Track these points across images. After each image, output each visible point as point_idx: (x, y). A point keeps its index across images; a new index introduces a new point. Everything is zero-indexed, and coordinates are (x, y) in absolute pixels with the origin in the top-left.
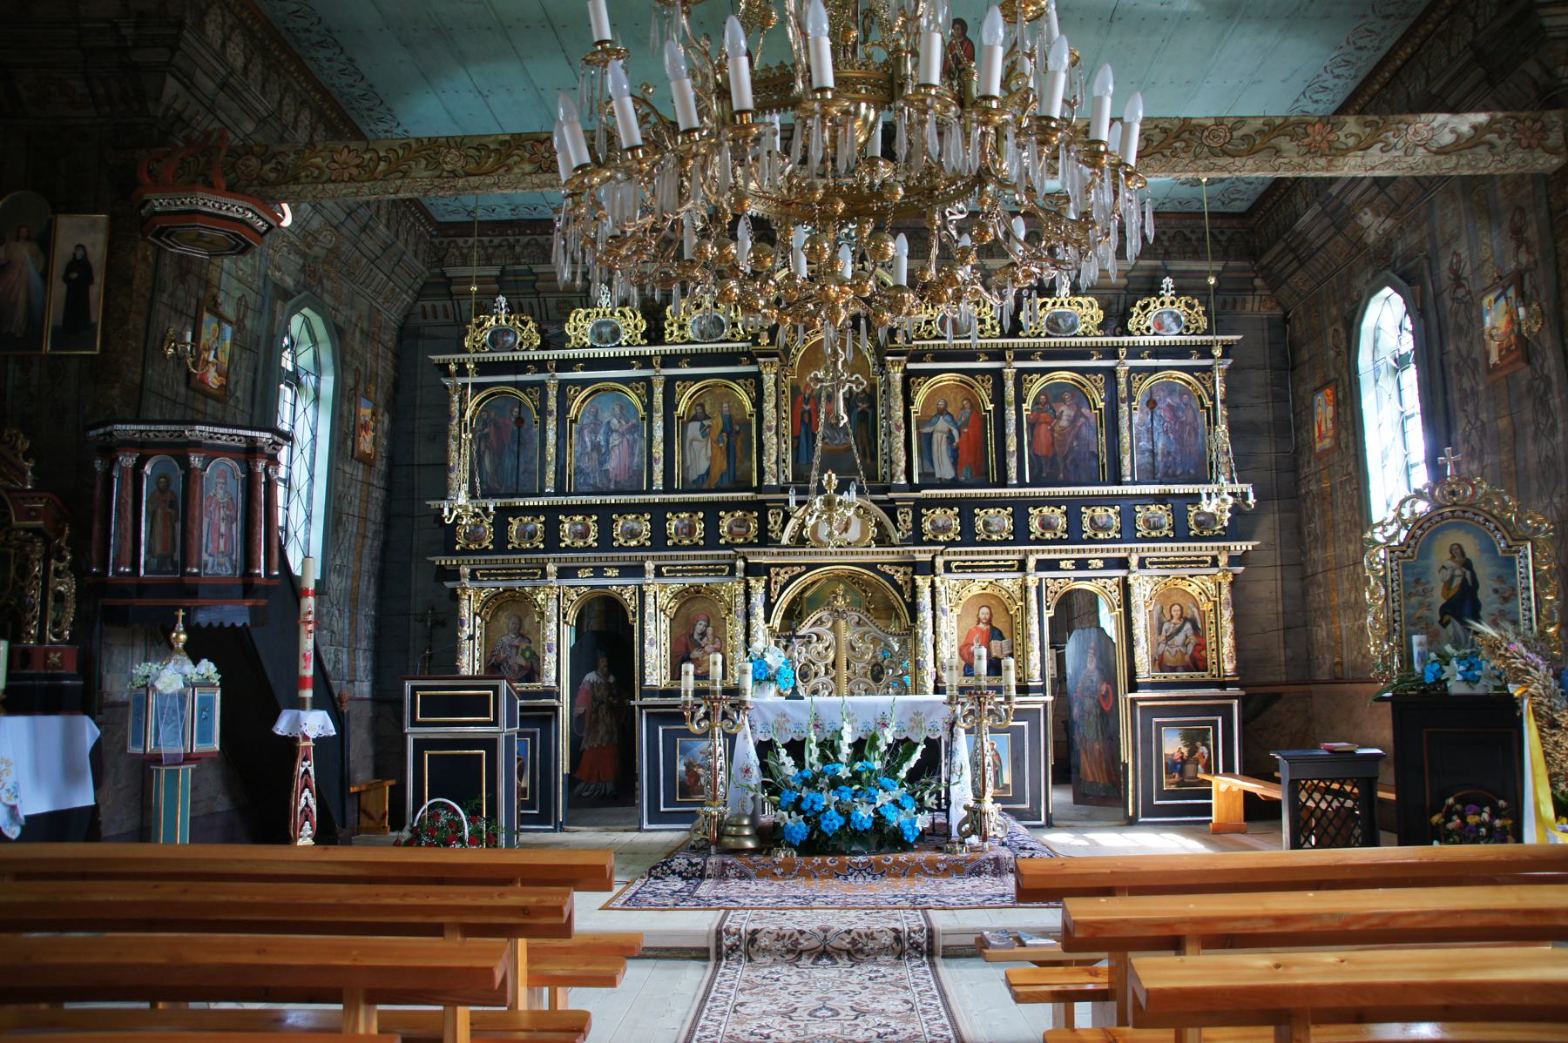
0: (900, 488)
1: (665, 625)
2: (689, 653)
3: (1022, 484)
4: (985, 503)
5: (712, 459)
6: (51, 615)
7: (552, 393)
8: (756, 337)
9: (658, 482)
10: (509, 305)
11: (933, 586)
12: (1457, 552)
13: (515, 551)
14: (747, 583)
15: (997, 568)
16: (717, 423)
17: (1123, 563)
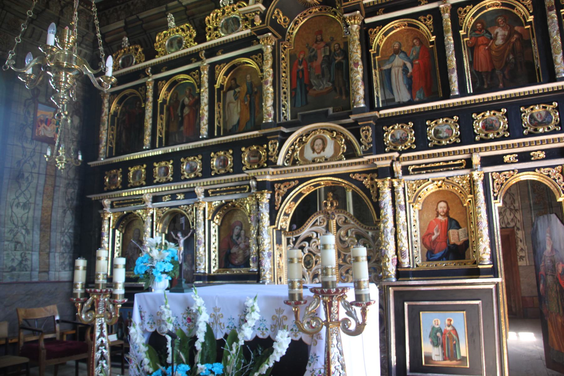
0: (362, 110)
5: (241, 113)
7: (150, 87)
10: (129, 41)
15: (447, 167)
16: (243, 89)
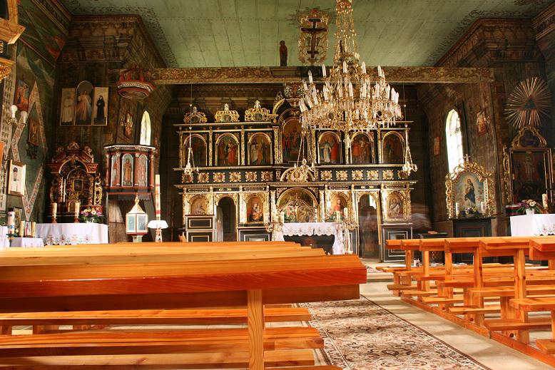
1: (245, 205)
2: (252, 213)
3: (350, 164)
4: (339, 169)
6: (95, 198)
8: (272, 121)
9: (243, 163)
11: (324, 194)
12: (469, 181)
13: (200, 183)
14: (270, 193)
16: (260, 145)
17: (379, 187)
